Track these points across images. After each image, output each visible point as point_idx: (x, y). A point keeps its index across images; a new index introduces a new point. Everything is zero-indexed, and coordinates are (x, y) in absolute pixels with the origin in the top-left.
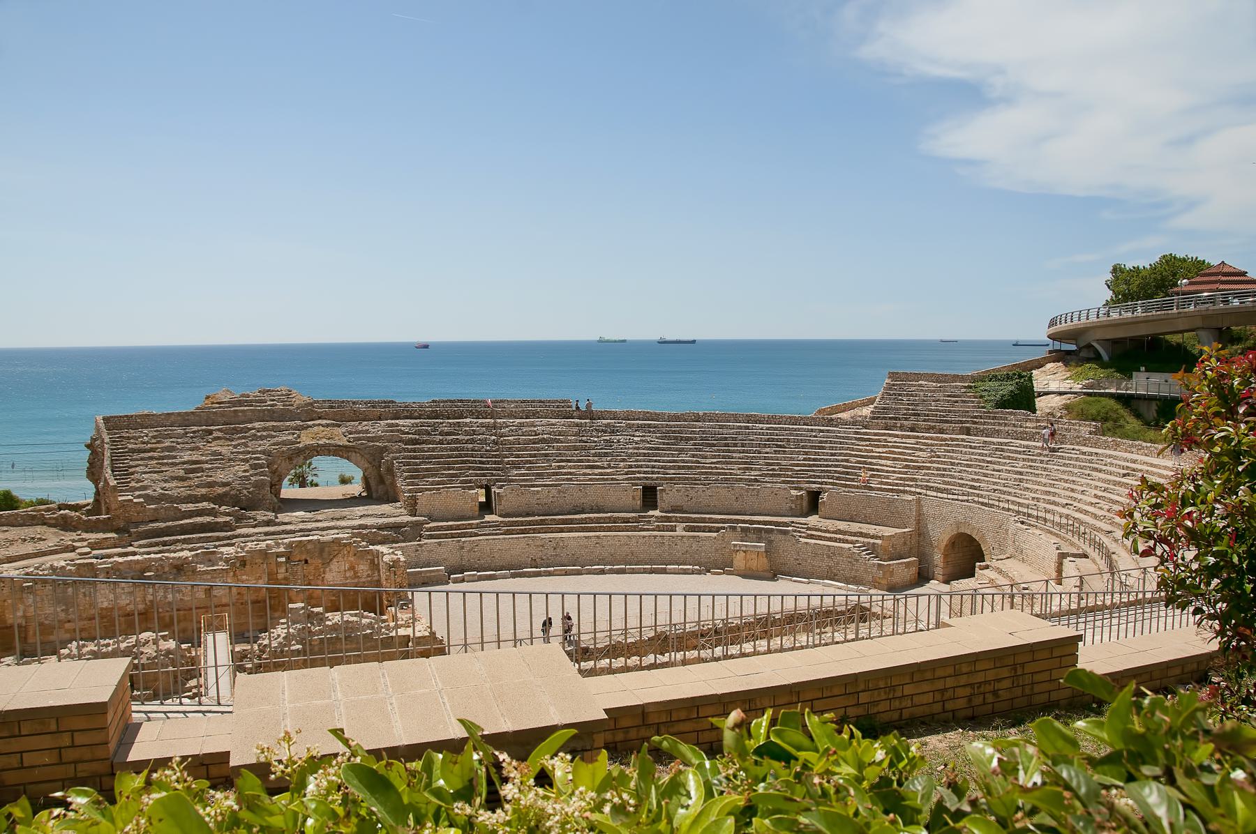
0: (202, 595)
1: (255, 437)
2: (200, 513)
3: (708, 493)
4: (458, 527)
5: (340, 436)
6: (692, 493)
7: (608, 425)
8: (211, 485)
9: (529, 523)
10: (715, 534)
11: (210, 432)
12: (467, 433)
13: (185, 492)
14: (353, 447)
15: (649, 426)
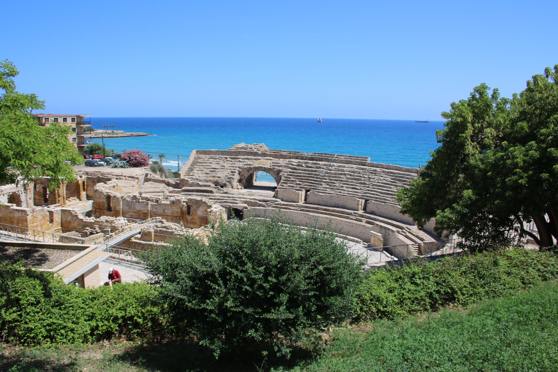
0: (162, 211)
1: (239, 161)
2: (205, 186)
3: (385, 207)
4: (286, 205)
5: (267, 163)
6: (379, 207)
7: (375, 170)
8: (214, 177)
9: (313, 208)
10: (370, 226)
11: (226, 158)
12: (317, 168)
13: (205, 178)
14: (270, 169)
15: (392, 173)
